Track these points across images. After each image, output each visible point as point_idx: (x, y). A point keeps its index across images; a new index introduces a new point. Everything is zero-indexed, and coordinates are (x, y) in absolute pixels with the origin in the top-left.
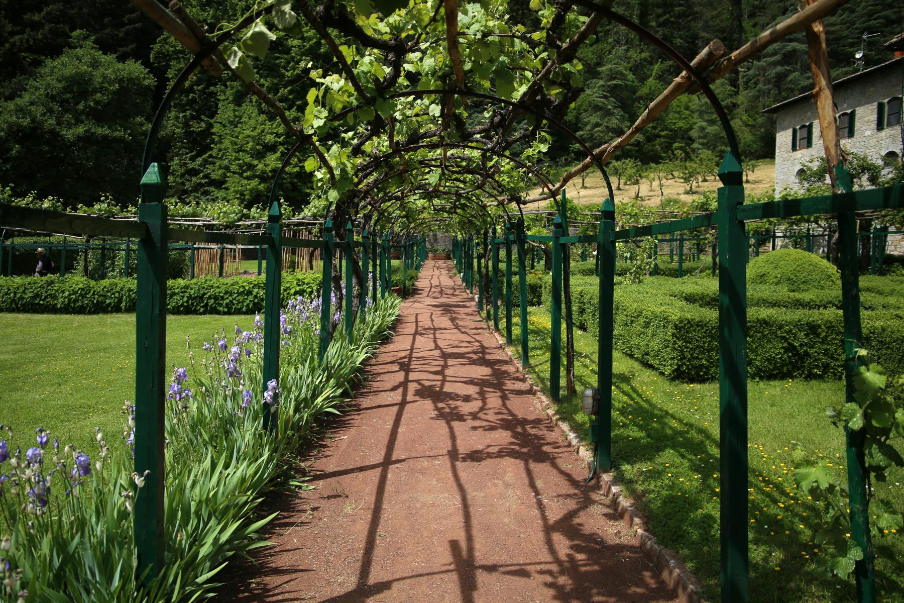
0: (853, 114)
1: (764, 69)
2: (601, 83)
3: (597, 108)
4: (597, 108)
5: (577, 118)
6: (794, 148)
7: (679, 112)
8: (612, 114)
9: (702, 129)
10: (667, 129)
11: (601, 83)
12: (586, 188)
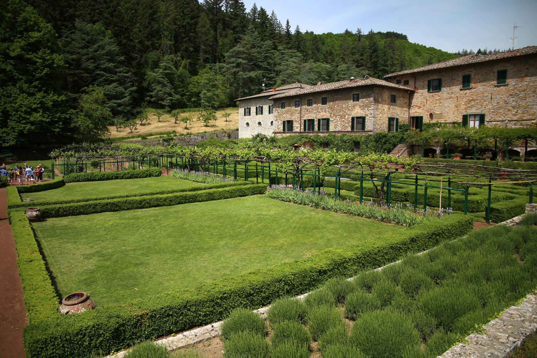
0: (262, 107)
1: (229, 69)
2: (161, 71)
3: (159, 82)
4: (159, 82)
5: (149, 84)
6: (245, 115)
7: (194, 85)
8: (166, 86)
9: (205, 94)
10: (189, 91)
11: (161, 71)
12: (160, 122)
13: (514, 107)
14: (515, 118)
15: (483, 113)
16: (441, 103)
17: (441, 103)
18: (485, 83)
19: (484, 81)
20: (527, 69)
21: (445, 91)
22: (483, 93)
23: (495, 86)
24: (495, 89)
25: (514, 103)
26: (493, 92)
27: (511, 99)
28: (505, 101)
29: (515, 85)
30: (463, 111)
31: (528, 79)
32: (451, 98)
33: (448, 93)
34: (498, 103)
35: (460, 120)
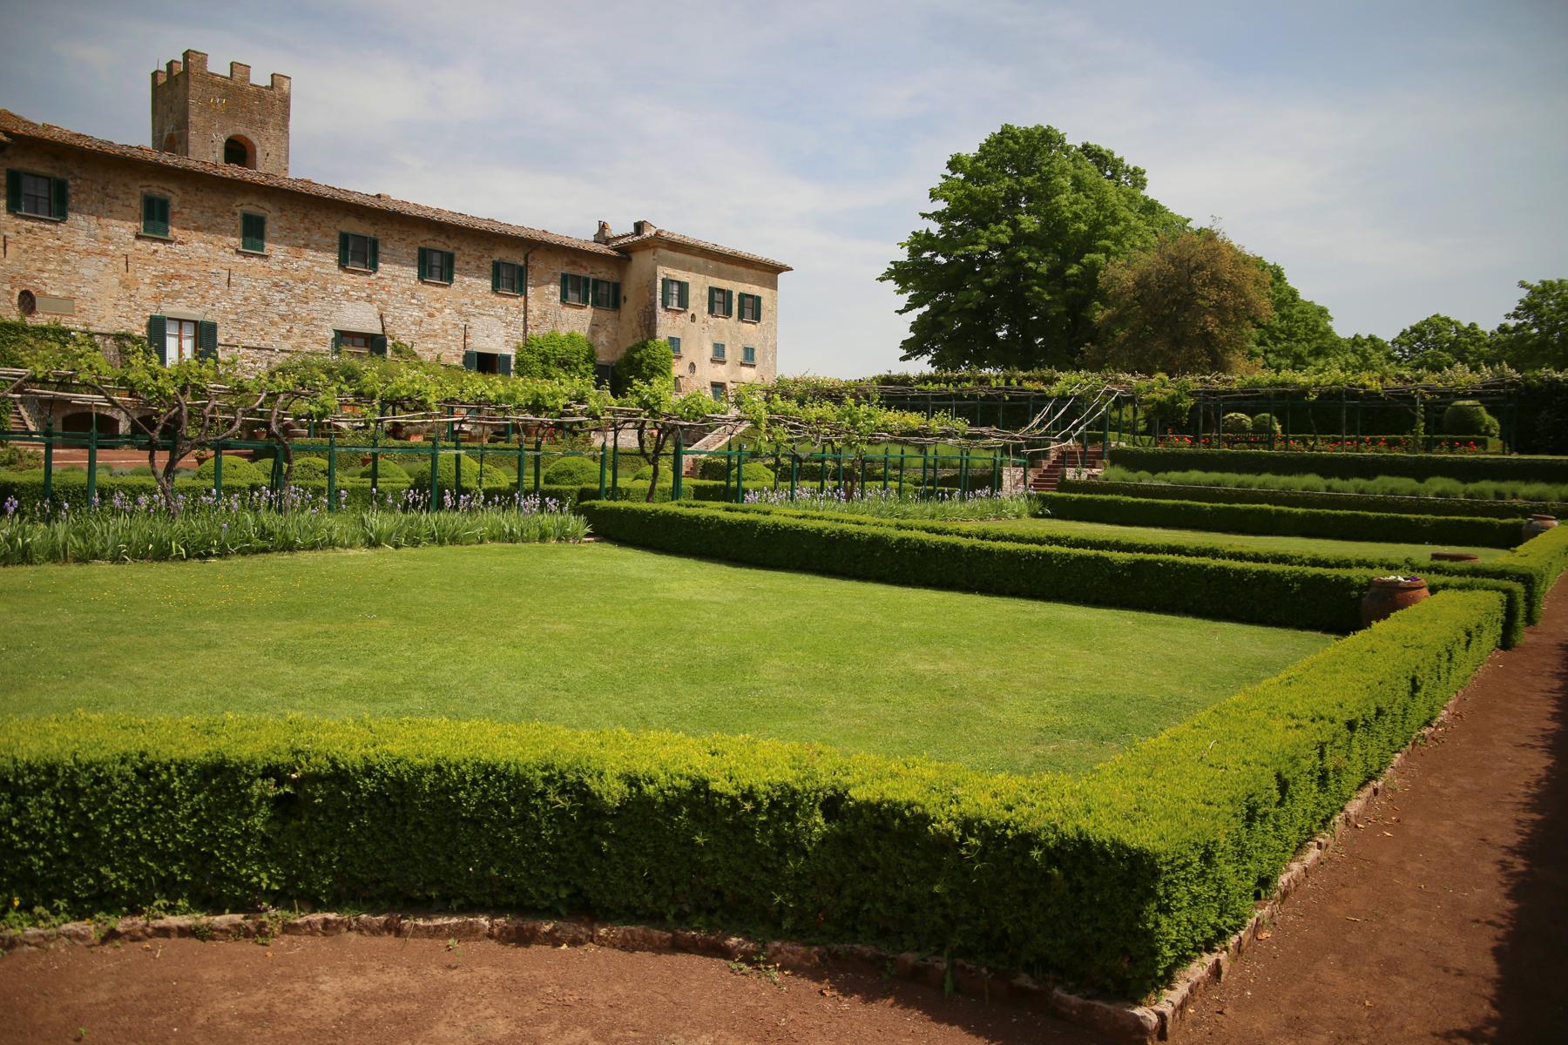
13: (283, 318)
14: (287, 346)
15: (209, 318)
16: (66, 262)
17: (66, 262)
18: (211, 237)
19: (209, 229)
20: (307, 229)
21: (80, 229)
22: (206, 263)
23: (238, 252)
24: (238, 259)
25: (283, 308)
26: (232, 266)
27: (278, 296)
28: (264, 299)
29: (283, 262)
30: (147, 304)
31: (309, 254)
32: (104, 253)
33: (94, 237)
34: (246, 299)
35: (140, 331)
